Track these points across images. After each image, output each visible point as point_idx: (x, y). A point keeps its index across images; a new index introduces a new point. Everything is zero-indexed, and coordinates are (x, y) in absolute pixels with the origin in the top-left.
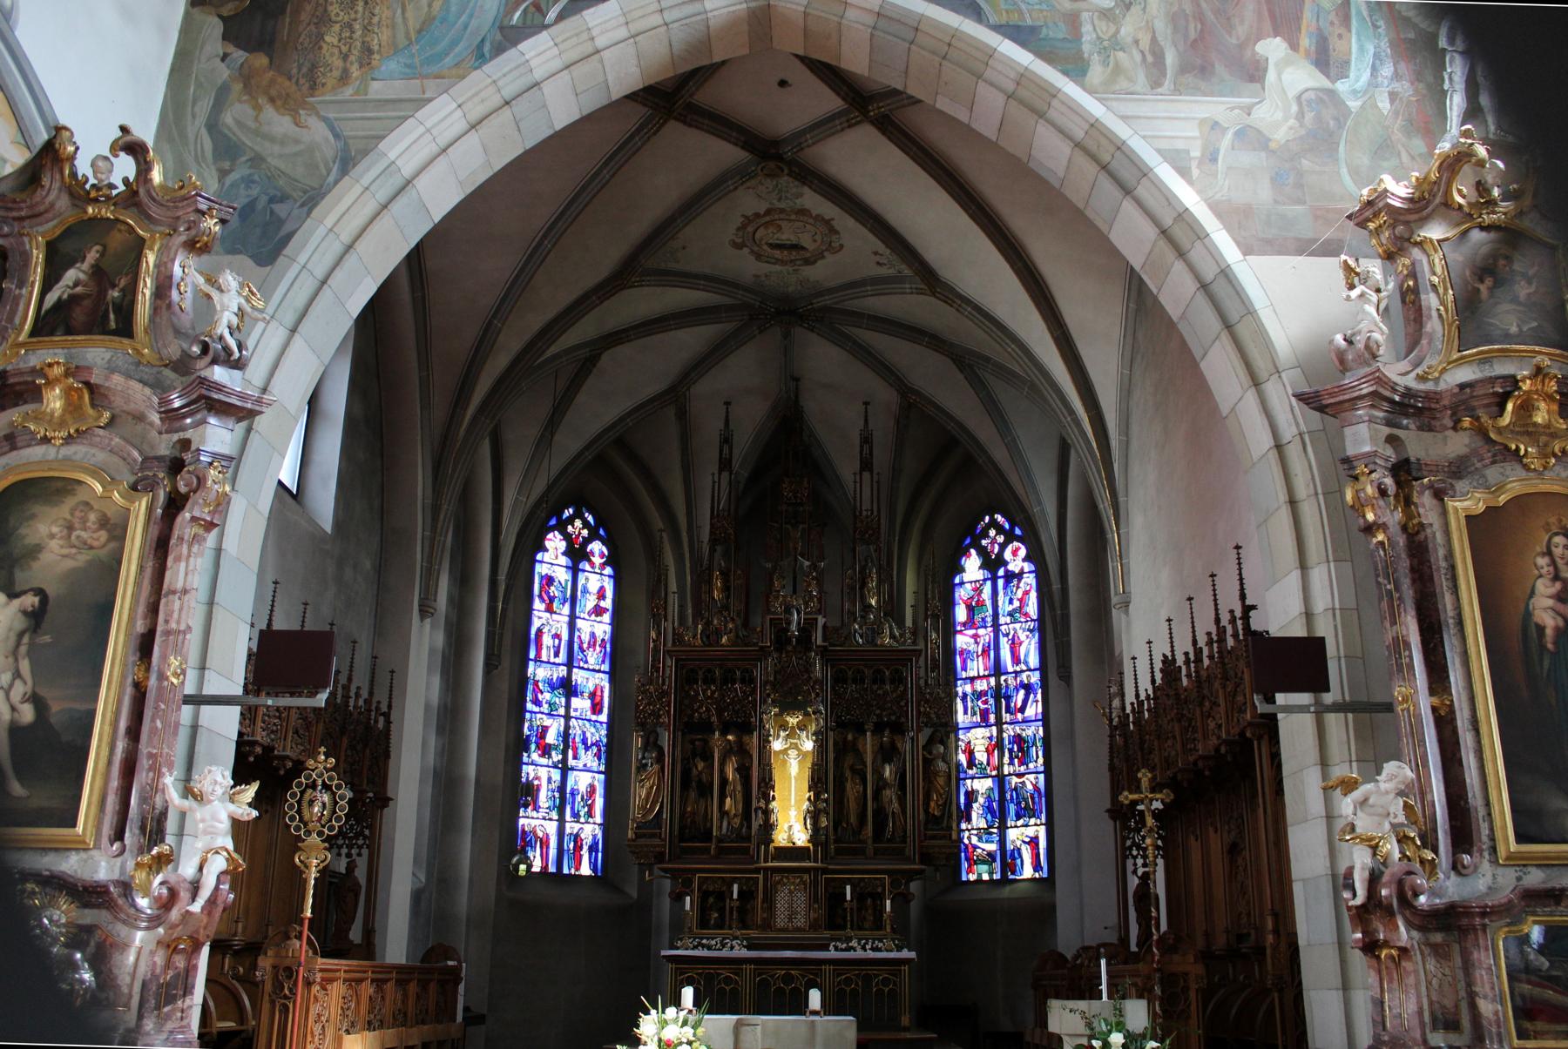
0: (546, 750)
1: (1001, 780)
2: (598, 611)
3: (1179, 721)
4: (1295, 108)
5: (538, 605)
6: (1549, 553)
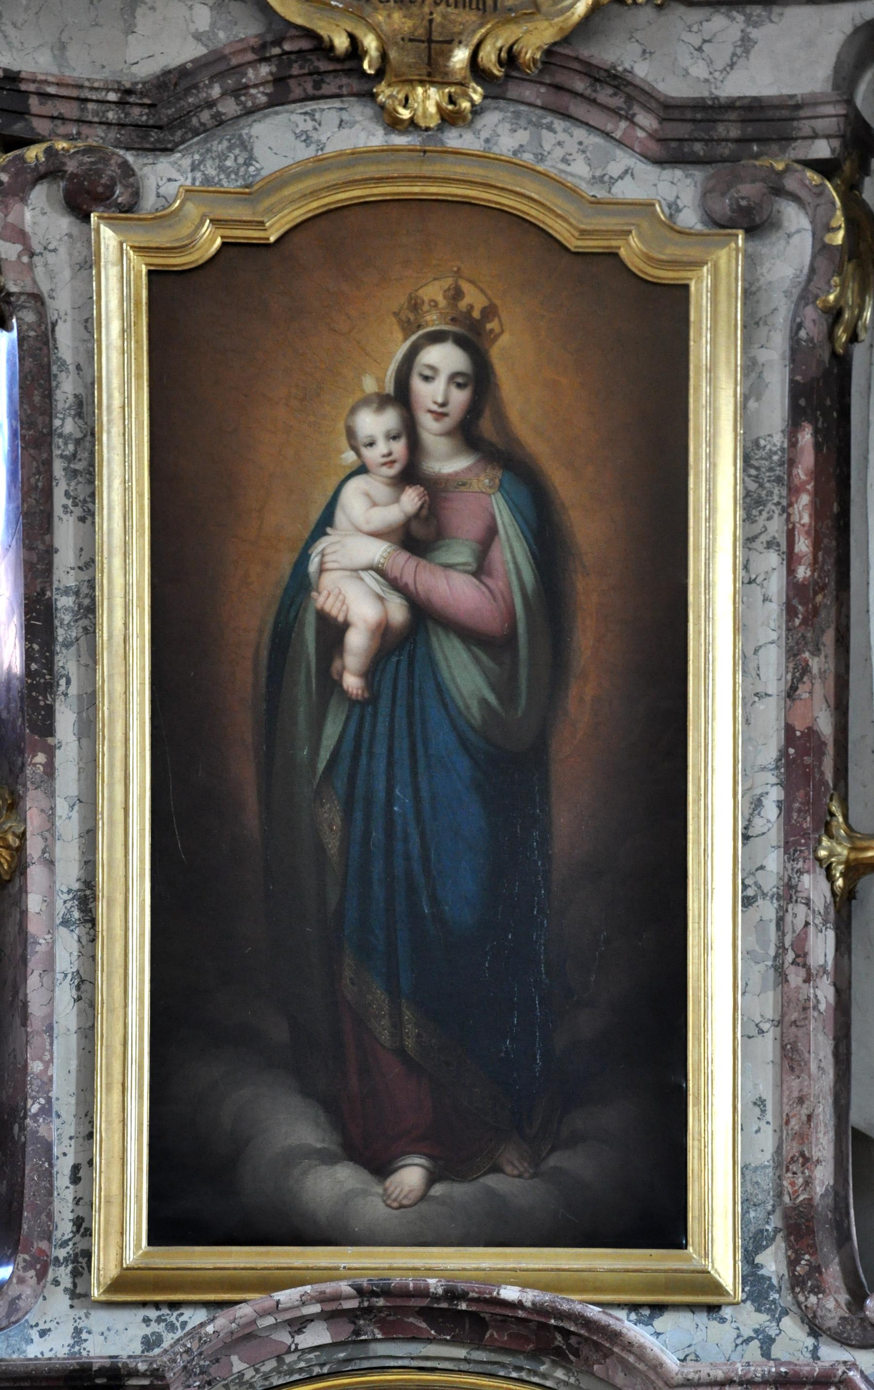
6: (401, 397)
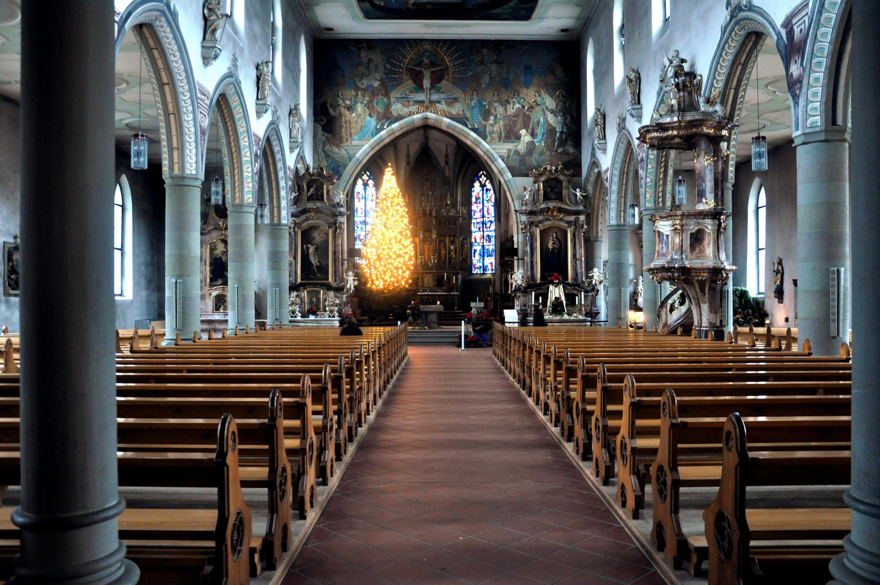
0: (361, 240)
1: (483, 247)
2: (372, 200)
5: (356, 200)
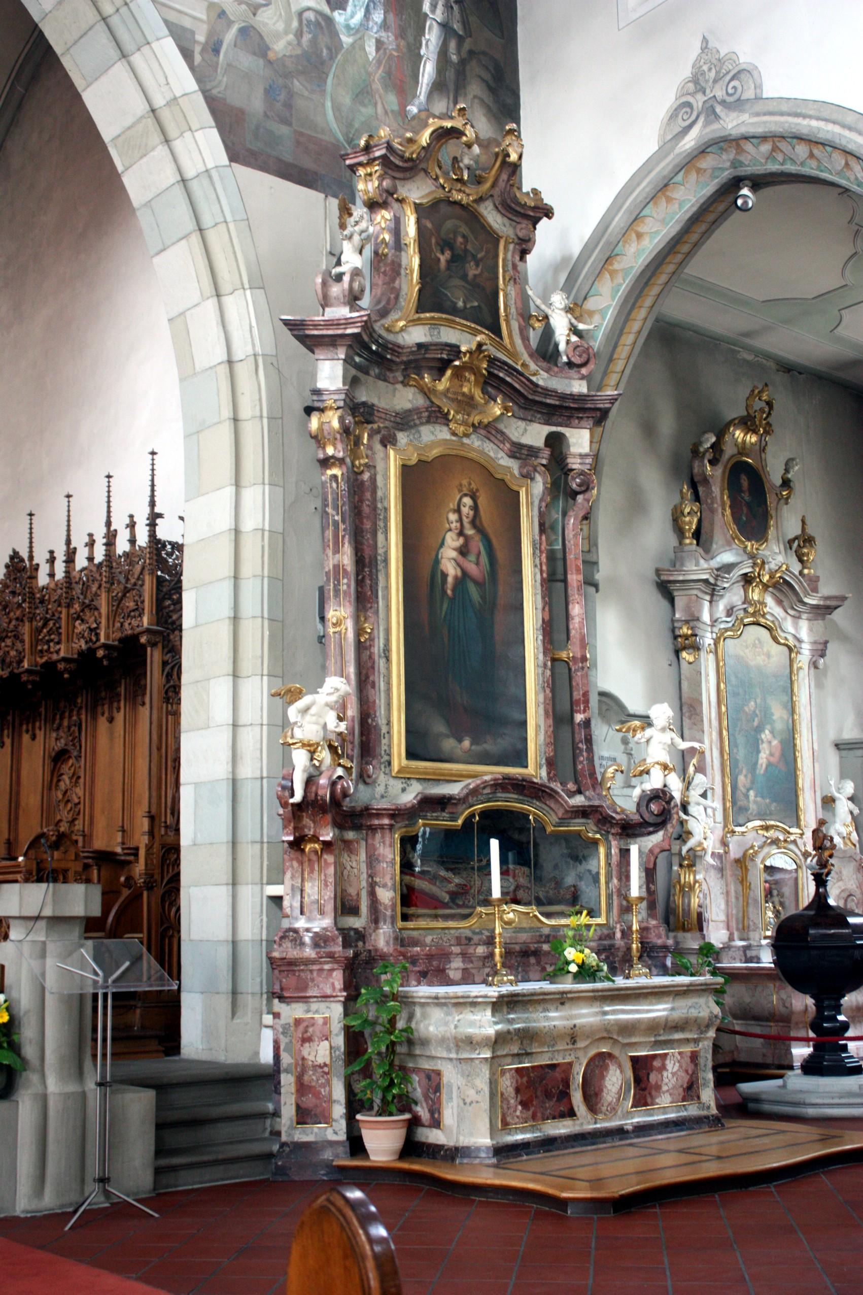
3: (31, 620)
4: (295, 24)
6: (458, 511)
